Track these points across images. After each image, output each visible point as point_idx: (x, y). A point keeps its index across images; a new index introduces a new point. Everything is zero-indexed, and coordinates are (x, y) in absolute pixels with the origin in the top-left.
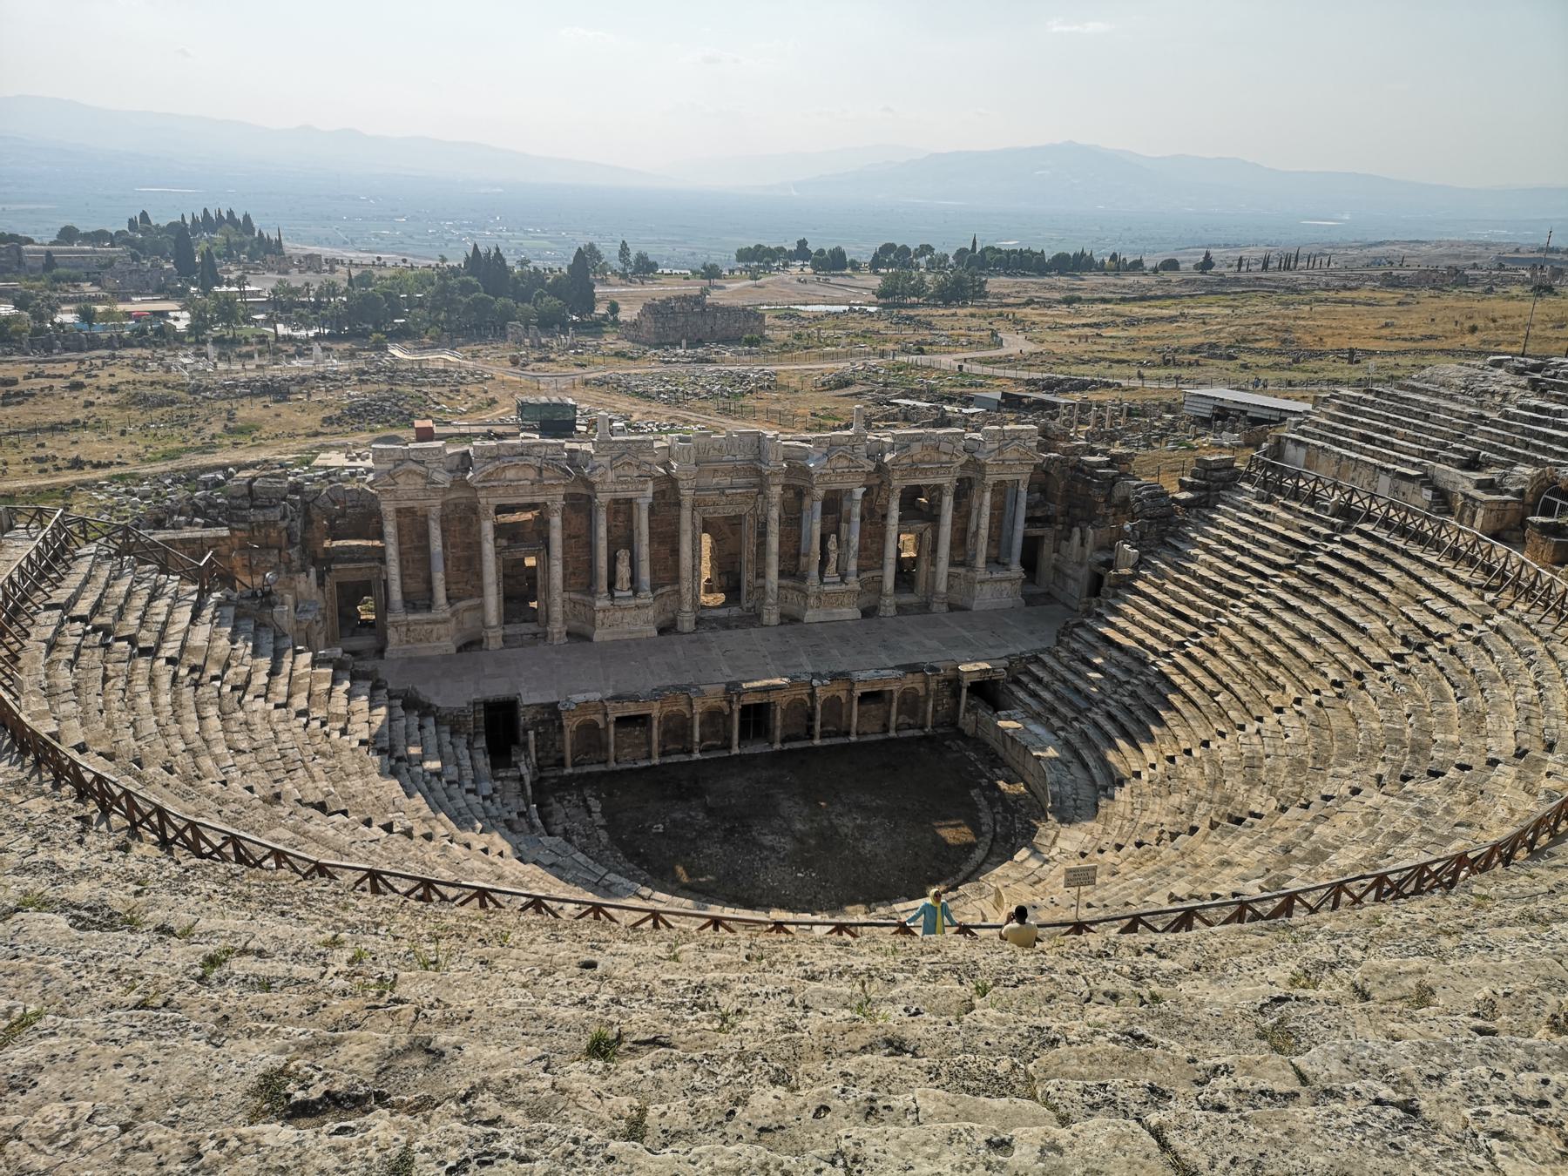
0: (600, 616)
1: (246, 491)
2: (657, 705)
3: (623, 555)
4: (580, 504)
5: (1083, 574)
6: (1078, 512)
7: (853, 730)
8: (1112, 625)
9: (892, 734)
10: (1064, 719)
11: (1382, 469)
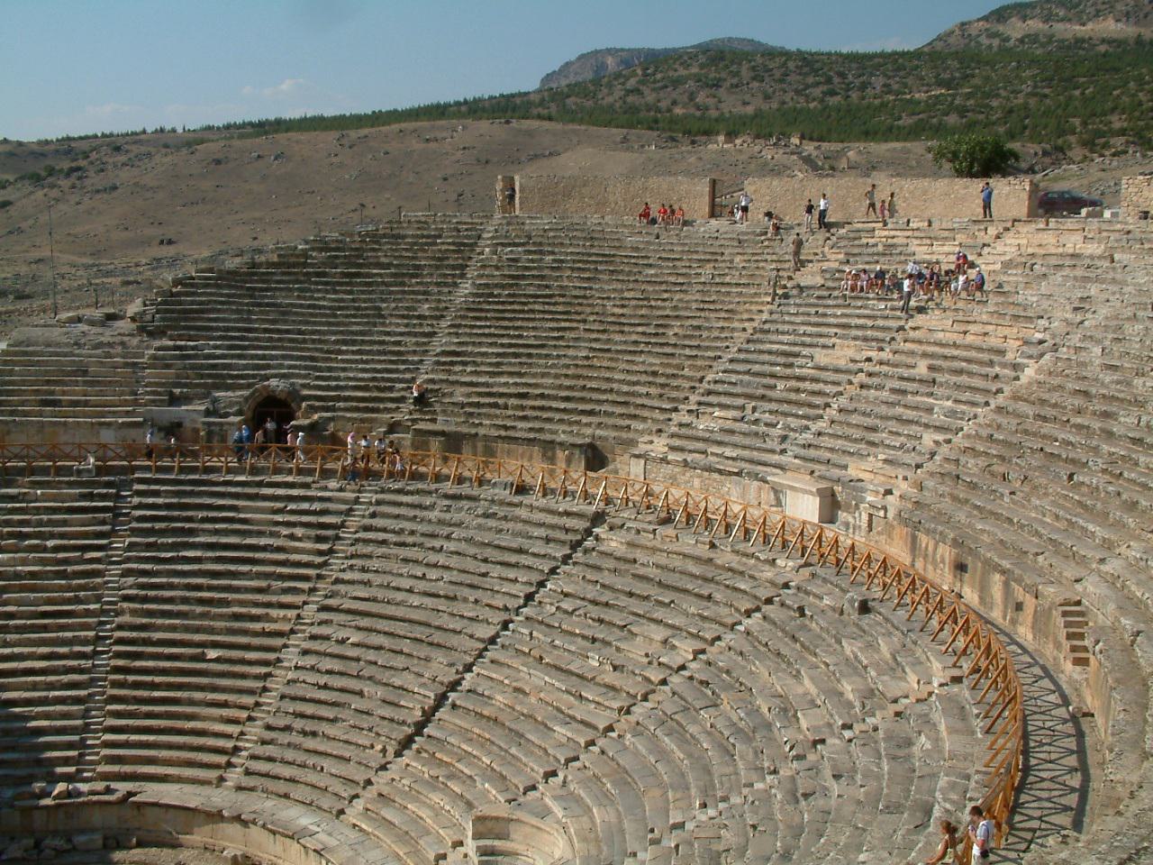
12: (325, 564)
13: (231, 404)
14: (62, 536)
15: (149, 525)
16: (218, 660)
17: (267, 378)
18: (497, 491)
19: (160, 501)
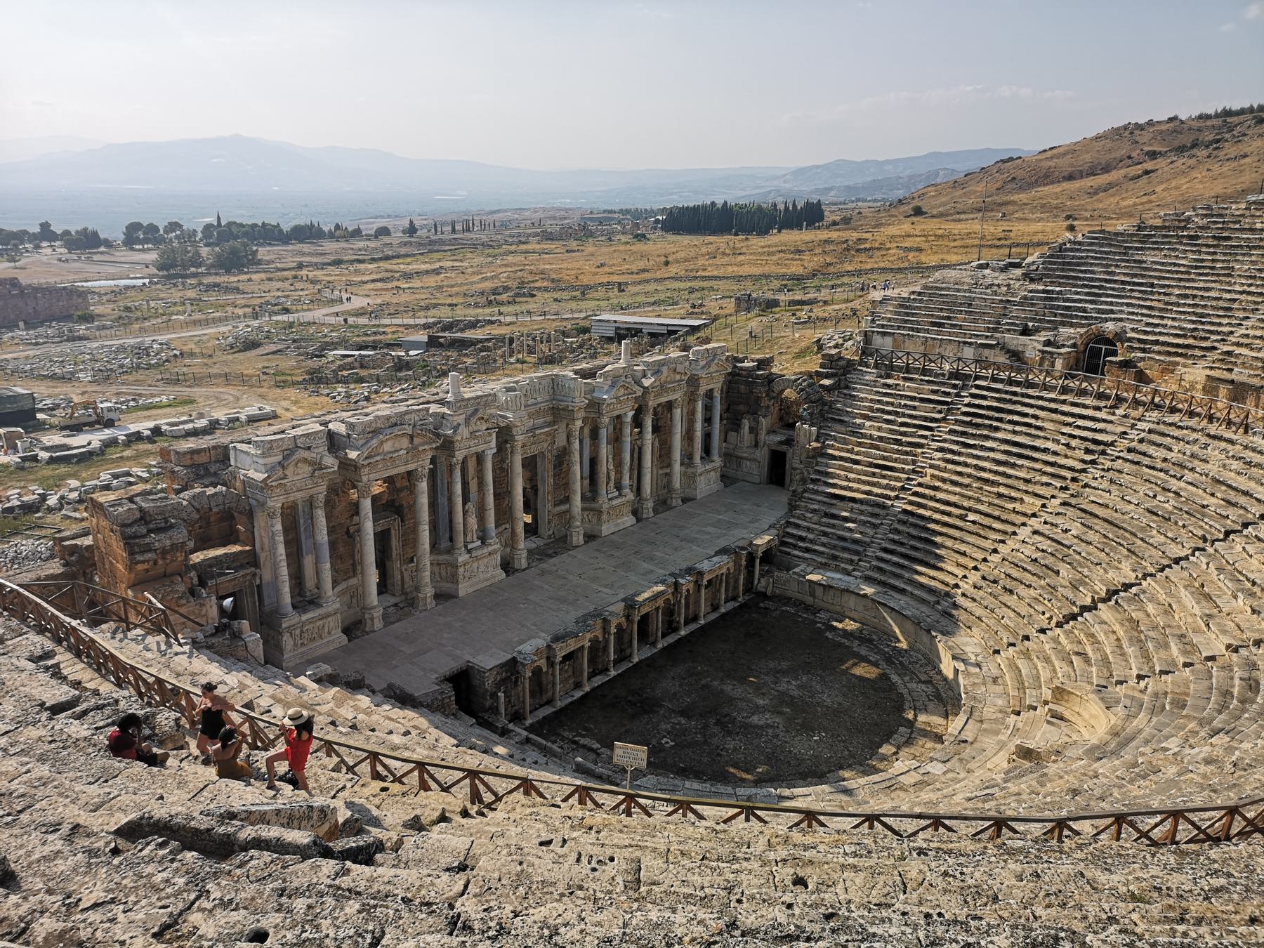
0: (461, 570)
5: (762, 455)
6: (742, 408)
8: (834, 486)
9: (723, 610)
10: (851, 562)
11: (965, 343)
12: (1084, 471)
13: (1069, 338)
14: (911, 416)
15: (968, 419)
16: (974, 522)
17: (1107, 320)
18: (1256, 439)
19: (984, 403)
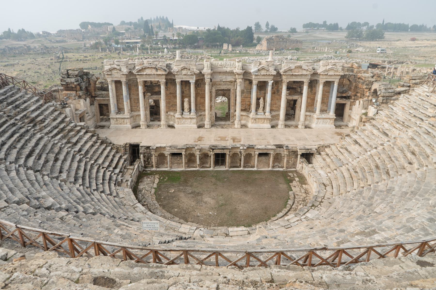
1: (66, 72)
2: (184, 150)
3: (186, 100)
4: (170, 81)
7: (256, 166)
